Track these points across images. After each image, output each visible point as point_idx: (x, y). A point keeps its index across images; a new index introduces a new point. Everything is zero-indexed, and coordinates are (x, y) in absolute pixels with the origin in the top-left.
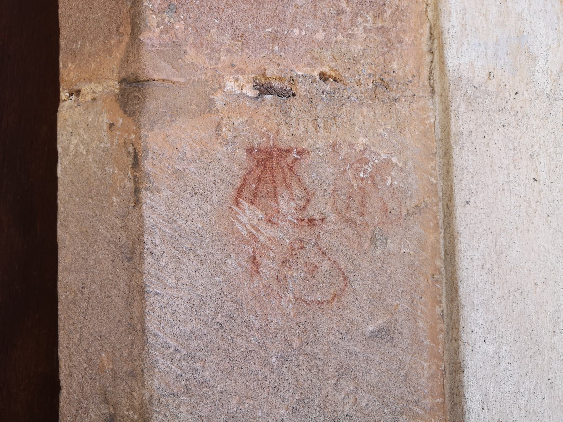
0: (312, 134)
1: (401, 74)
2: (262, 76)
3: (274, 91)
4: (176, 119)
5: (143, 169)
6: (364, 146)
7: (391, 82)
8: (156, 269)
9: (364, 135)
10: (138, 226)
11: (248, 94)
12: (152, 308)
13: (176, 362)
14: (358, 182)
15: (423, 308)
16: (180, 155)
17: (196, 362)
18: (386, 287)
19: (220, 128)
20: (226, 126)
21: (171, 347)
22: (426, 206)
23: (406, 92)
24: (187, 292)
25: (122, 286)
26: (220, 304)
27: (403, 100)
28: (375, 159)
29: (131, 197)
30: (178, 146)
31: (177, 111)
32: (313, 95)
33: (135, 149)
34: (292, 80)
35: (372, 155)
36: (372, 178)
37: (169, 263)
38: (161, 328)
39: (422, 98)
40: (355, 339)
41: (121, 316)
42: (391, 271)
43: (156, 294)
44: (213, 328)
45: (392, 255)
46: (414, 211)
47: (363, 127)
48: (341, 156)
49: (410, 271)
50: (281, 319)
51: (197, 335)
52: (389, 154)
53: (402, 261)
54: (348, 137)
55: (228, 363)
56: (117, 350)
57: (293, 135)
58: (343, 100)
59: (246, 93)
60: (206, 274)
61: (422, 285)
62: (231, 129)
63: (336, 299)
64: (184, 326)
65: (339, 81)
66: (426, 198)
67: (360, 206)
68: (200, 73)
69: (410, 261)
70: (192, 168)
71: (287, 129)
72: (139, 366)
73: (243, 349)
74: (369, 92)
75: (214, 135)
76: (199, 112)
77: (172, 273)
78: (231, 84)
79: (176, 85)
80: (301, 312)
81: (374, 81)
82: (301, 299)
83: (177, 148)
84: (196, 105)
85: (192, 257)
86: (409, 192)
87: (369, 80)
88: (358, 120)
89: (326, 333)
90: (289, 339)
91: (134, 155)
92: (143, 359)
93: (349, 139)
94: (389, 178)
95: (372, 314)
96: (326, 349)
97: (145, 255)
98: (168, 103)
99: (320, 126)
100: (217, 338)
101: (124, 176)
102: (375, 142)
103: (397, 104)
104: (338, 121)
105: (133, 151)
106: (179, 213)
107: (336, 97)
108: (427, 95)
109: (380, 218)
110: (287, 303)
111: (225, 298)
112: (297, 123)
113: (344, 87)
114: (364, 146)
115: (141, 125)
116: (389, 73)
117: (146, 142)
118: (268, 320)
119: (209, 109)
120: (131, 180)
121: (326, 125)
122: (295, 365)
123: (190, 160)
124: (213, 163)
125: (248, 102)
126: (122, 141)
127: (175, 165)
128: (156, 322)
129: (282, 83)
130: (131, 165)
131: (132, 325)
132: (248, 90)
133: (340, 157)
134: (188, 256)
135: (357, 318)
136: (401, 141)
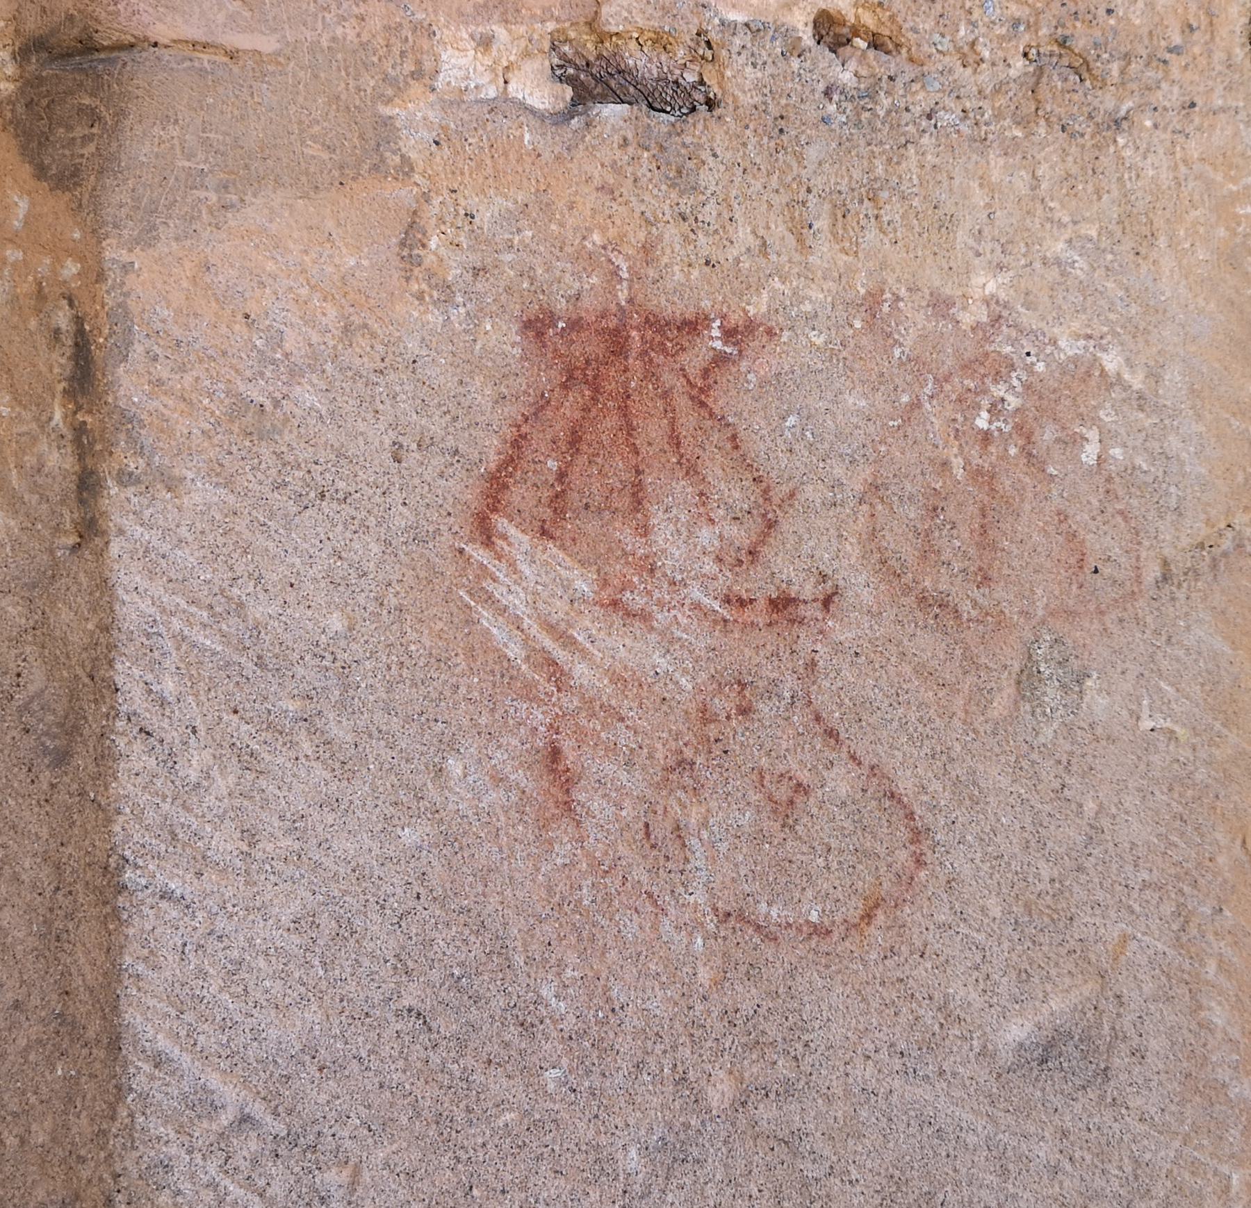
0: (784, 258)
1: (1137, 22)
2: (587, 29)
3: (632, 89)
4: (242, 201)
5: (110, 400)
6: (993, 306)
7: (1099, 52)
8: (164, 797)
9: (990, 262)
10: (90, 626)
11: (529, 101)
12: (146, 952)
13: (243, 1165)
14: (967, 449)
15: (1228, 952)
16: (258, 343)
17: (324, 1168)
18: (1080, 869)
19: (419, 236)
20: (443, 228)
21: (223, 1107)
22: (1240, 546)
23: (1159, 94)
24: (288, 886)
25: (27, 865)
26: (417, 935)
27: (1148, 123)
28: (1034, 359)
29: (66, 512)
30: (253, 308)
31: (247, 167)
32: (787, 105)
33: (78, 320)
34: (703, 44)
35: (1024, 342)
36: (1025, 433)
37: (215, 773)
38: (183, 1033)
39: (1222, 115)
40: (954, 1074)
41: (23, 982)
42: (1101, 805)
43: (162, 897)
44: (389, 1033)
45: (1104, 743)
46: (1189, 565)
47: (986, 233)
48: (901, 345)
49: (1174, 804)
50: (660, 994)
51: (325, 1060)
52: (1089, 337)
53: (1142, 767)
54: (928, 272)
55: (449, 1172)
56: (9, 1118)
57: (707, 263)
58: (907, 125)
59: (520, 97)
60: (363, 815)
61: (1221, 860)
62: (463, 239)
63: (880, 918)
64: (277, 1022)
65: (891, 46)
66: (1238, 515)
67: (977, 544)
68: (338, 15)
69: (1176, 766)
70: (307, 395)
71: (686, 239)
72: (95, 1181)
73: (509, 1116)
74: (1011, 94)
75: (396, 261)
76: (336, 173)
77: (225, 812)
78: (462, 61)
79: (241, 63)
80: (743, 969)
81: (1030, 47)
82: (741, 917)
83: (247, 317)
84: (323, 145)
85: (307, 747)
86: (1173, 489)
87: (1014, 43)
88: (967, 202)
89: (840, 1052)
90: (691, 1075)
91: (76, 344)
92: (110, 1156)
93: (932, 278)
94: (1093, 435)
95: (1024, 976)
96: (840, 1114)
97: (121, 742)
98: (212, 136)
99: (815, 227)
100: (404, 1071)
101: (34, 425)
102: (1035, 291)
103: (1121, 141)
104: (888, 207)
105: (72, 328)
106: (256, 575)
107: (882, 113)
108: (1241, 104)
109: (1057, 593)
110: (683, 933)
111: (438, 913)
112: (726, 216)
113: (910, 72)
114: (993, 306)
115: (105, 223)
116: (1090, 17)
117: (125, 289)
118: (609, 1000)
119: (376, 159)
120: (63, 442)
121: (840, 224)
122: (718, 1177)
123: (300, 362)
124: (392, 376)
125: (530, 131)
126: (27, 286)
127: (239, 383)
128: (162, 1007)
129: (664, 57)
130: (64, 384)
131: (70, 1019)
132: (528, 83)
133: (897, 352)
134: (292, 744)
135: (962, 991)
136: (1137, 286)
